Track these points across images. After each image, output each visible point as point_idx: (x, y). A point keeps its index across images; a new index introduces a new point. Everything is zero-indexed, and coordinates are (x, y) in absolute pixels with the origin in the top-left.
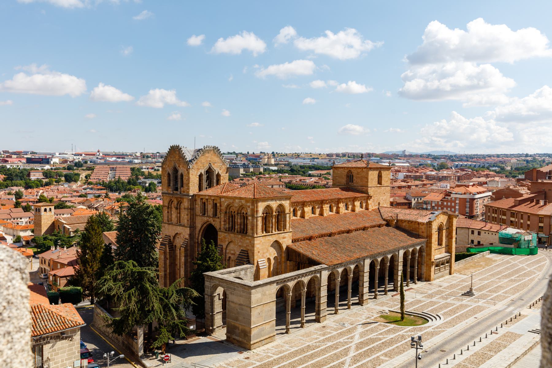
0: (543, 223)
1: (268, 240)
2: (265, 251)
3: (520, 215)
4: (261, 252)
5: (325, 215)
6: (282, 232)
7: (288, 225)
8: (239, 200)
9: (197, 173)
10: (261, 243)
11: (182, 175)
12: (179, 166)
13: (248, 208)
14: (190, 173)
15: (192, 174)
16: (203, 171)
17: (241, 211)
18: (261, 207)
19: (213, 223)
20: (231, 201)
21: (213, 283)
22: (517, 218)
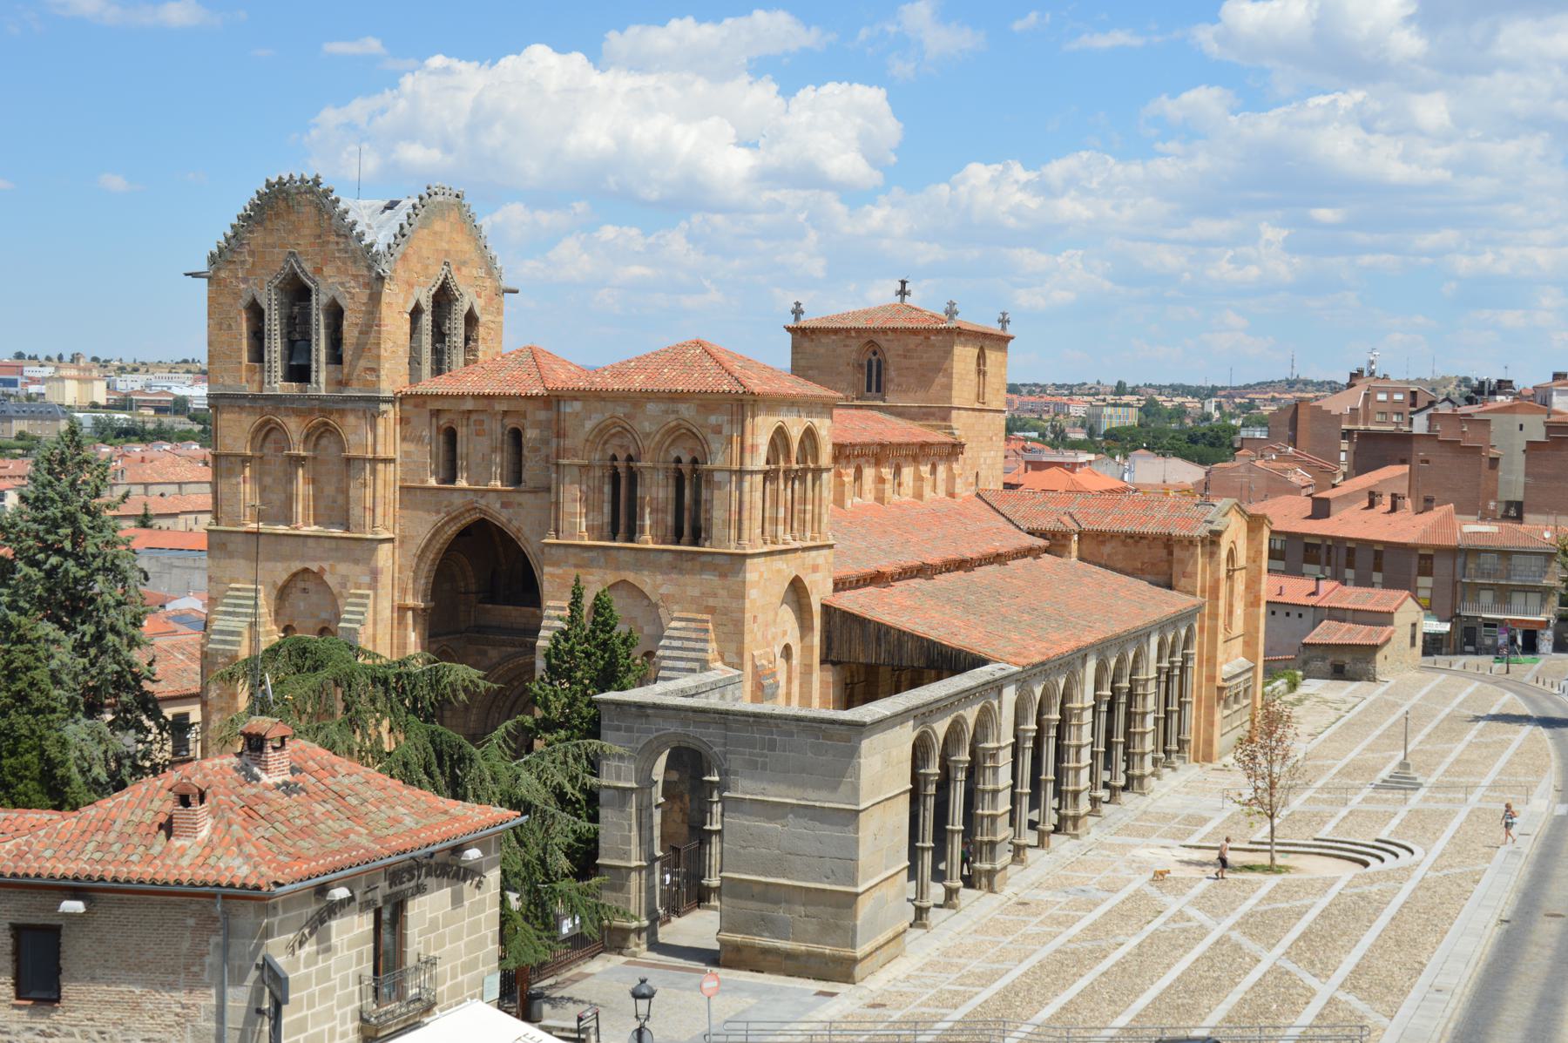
0: (1430, 574)
1: (779, 571)
2: (771, 616)
3: (1343, 553)
4: (760, 620)
5: (848, 504)
6: (810, 544)
7: (825, 519)
8: (662, 406)
9: (406, 302)
10: (762, 582)
11: (336, 314)
12: (319, 270)
13: (710, 437)
14: (385, 299)
15: (390, 304)
16: (425, 298)
17: (667, 451)
18: (761, 430)
19: (502, 516)
20: (620, 411)
21: (649, 731)
22: (1328, 564)
